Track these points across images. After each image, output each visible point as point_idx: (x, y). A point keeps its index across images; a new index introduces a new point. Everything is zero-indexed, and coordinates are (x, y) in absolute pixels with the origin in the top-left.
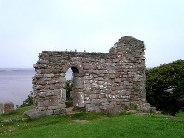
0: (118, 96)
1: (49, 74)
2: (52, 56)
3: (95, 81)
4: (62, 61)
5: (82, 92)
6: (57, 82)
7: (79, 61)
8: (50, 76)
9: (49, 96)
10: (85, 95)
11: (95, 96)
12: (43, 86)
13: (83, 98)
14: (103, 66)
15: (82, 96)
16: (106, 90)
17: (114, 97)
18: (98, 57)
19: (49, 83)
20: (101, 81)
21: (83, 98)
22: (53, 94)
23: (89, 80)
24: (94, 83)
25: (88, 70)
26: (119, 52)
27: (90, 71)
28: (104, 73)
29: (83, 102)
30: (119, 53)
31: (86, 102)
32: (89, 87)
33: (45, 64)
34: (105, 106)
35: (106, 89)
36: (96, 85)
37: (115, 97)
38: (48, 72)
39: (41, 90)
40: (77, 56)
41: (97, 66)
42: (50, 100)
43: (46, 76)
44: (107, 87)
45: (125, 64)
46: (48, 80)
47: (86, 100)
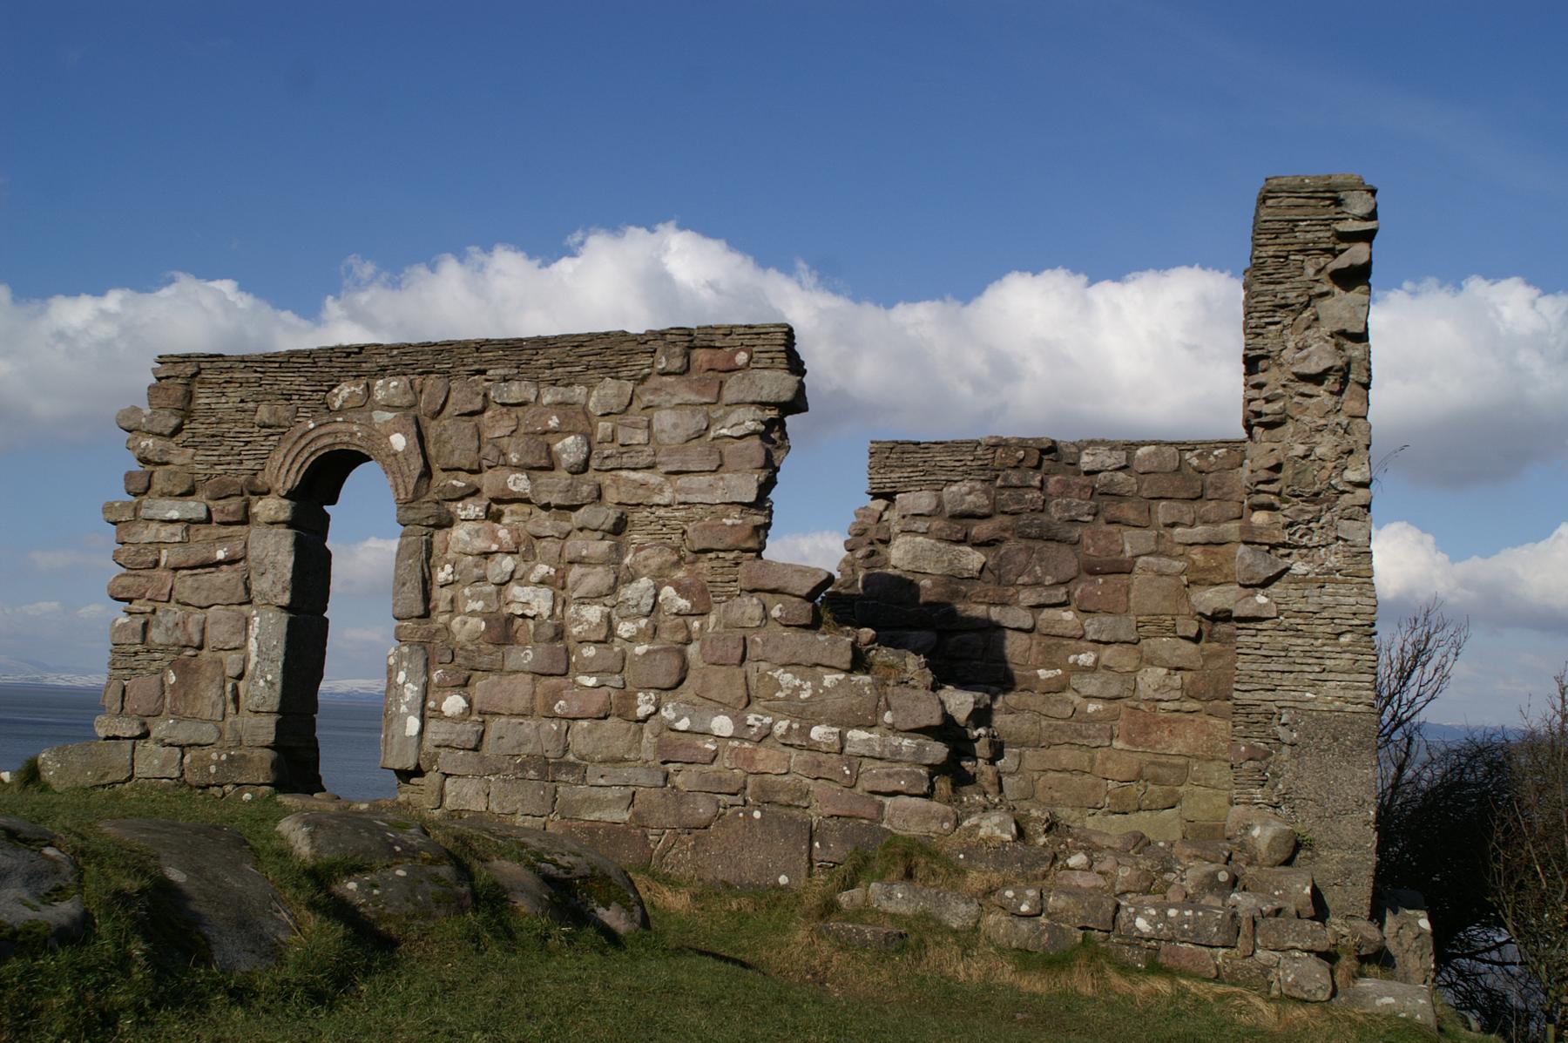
1: (166, 502)
3: (532, 569)
4: (264, 413)
5: (405, 649)
6: (220, 555)
7: (389, 407)
8: (175, 515)
11: (519, 690)
13: (408, 696)
16: (640, 650)
18: (563, 364)
19: (174, 561)
20: (583, 570)
21: (411, 691)
23: (486, 555)
29: (413, 725)
32: (473, 613)
40: (382, 371)
41: (549, 438)
47: (439, 714)
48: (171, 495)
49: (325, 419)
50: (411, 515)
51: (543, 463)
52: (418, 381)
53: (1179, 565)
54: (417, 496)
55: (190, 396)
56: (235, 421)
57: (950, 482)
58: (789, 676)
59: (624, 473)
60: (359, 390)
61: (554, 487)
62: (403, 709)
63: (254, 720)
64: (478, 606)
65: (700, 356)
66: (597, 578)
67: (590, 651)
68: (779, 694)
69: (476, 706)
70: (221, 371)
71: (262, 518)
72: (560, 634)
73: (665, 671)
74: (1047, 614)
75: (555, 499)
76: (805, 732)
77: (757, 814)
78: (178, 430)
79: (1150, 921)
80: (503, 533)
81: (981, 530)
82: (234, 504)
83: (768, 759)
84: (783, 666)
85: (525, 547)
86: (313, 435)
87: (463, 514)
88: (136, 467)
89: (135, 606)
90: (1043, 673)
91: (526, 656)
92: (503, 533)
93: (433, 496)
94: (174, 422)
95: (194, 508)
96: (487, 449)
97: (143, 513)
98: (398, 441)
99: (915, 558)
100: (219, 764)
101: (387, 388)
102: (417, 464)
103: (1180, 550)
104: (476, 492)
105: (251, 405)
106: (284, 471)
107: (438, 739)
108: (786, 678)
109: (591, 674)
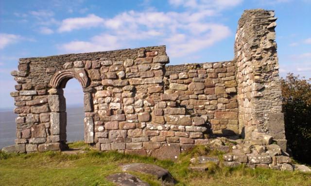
1: (27, 91)
4: (48, 70)
6: (41, 102)
7: (78, 67)
8: (29, 94)
15: (88, 124)
16: (141, 114)
18: (117, 56)
19: (29, 104)
23: (104, 97)
27: (103, 82)
29: (92, 134)
31: (98, 135)
32: (103, 109)
33: (20, 76)
34: (138, 143)
40: (75, 60)
41: (116, 72)
47: (98, 131)
48: (27, 90)
49: (63, 71)
50: (86, 90)
51: (115, 77)
53: (223, 85)
54: (87, 86)
55: (29, 68)
57: (179, 73)
58: (172, 117)
59: (133, 78)
61: (119, 82)
62: (89, 131)
63: (54, 136)
64: (104, 108)
65: (148, 53)
66: (130, 100)
67: (130, 115)
69: (106, 128)
70: (36, 61)
71: (50, 93)
72: (123, 112)
73: (147, 117)
74: (199, 95)
75: (119, 85)
76: (177, 127)
77: (169, 145)
78: (27, 75)
79: (255, 160)
80: (107, 92)
81: (185, 81)
82: (43, 91)
83: (170, 133)
85: (112, 95)
86: (61, 74)
88: (17, 84)
89: (21, 115)
90: (200, 106)
91: (116, 117)
93: (91, 86)
94: (25, 73)
95: (33, 92)
96: (102, 75)
97: (20, 94)
98: (82, 75)
99: (174, 87)
100: (47, 147)
101: (77, 63)
102: (86, 79)
104: (101, 85)
105: (45, 69)
106: (54, 82)
107: (99, 136)
108: (171, 116)
109: (131, 120)
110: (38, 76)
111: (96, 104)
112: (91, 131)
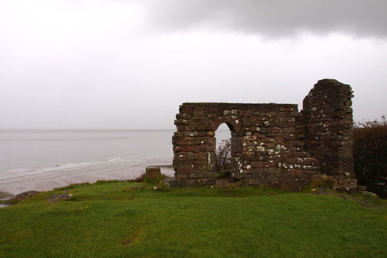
0: (299, 166)
2: (195, 109)
3: (260, 143)
4: (210, 116)
9: (191, 161)
10: (245, 162)
12: (183, 148)
14: (273, 122)
15: (239, 163)
17: (291, 167)
19: (191, 144)
22: (197, 158)
23: (251, 141)
24: (259, 146)
25: (249, 127)
26: (315, 102)
28: (274, 132)
30: (315, 104)
33: (185, 119)
35: (278, 155)
36: (263, 149)
37: (294, 166)
38: (190, 130)
39: (180, 153)
42: (193, 166)
43: (187, 135)
44: (279, 152)
45: (322, 120)
46: (189, 140)
47: (246, 169)
52: (239, 110)
56: (203, 117)
58: (300, 159)
59: (275, 128)
60: (229, 112)
62: (240, 168)
64: (251, 150)
68: (298, 161)
70: (200, 107)
77: (297, 180)
79: (349, 189)
80: (255, 138)
84: (299, 157)
87: (248, 134)
92: (255, 138)
100: (205, 181)
103: (297, 129)
105: (207, 114)
108: (300, 159)
109: (272, 161)
110: (201, 120)
111: (245, 146)
112: (241, 169)
